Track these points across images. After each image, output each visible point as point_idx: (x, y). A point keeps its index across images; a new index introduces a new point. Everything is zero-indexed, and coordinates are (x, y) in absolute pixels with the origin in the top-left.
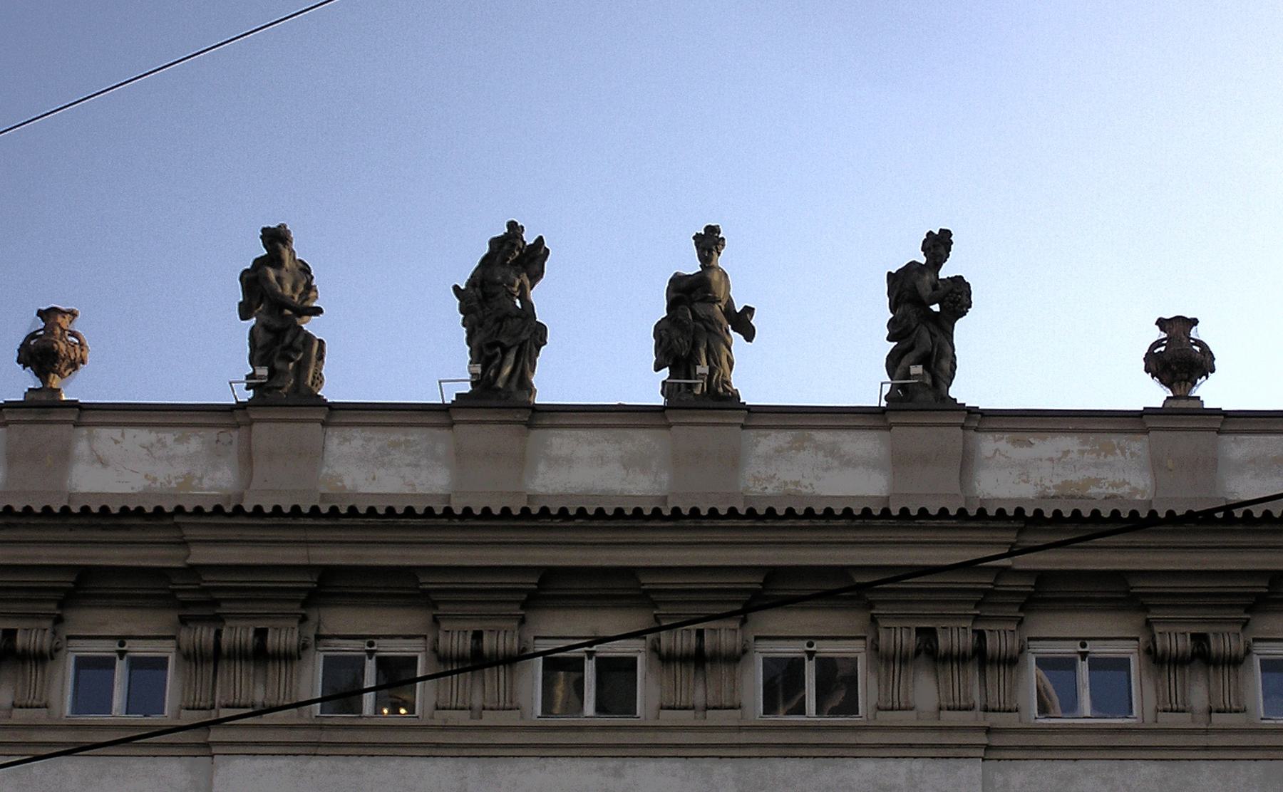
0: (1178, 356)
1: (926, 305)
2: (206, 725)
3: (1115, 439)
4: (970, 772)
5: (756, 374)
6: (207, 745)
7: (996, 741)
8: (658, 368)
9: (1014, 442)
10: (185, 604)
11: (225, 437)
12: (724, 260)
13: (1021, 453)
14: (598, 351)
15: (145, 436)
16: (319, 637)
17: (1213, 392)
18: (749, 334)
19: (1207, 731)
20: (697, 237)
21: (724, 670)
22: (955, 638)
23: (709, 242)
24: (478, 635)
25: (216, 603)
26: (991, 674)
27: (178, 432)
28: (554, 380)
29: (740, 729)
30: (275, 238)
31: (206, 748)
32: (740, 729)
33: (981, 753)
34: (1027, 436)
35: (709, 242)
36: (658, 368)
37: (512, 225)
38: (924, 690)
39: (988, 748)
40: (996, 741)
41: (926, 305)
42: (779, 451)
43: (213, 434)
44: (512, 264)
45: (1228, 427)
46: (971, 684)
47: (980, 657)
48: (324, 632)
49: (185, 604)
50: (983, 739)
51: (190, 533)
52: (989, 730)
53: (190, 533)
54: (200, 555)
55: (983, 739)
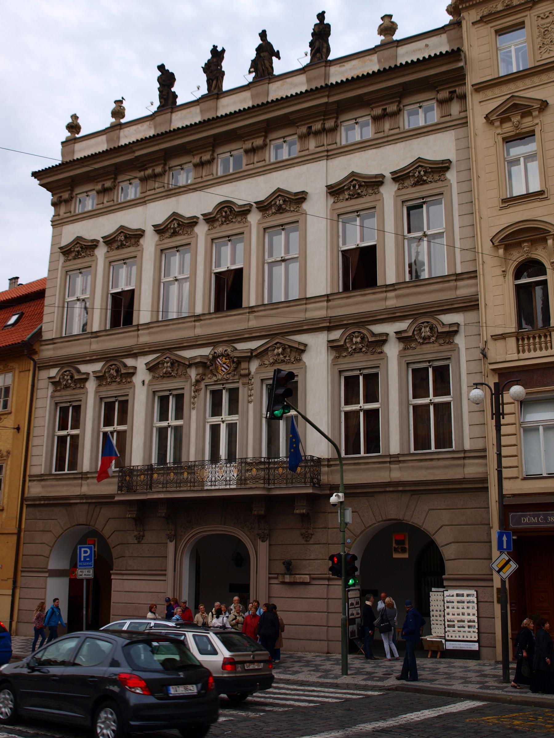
0: (388, 27)
1: (321, 33)
2: (145, 197)
3: (367, 58)
4: (323, 163)
5: (279, 67)
6: (145, 202)
7: (329, 153)
8: (250, 72)
9: (340, 66)
10: (140, 167)
11: (151, 123)
12: (269, 39)
13: (343, 69)
14: (237, 73)
15: (134, 128)
16: (170, 168)
17: (397, 36)
18: (279, 58)
19: (387, 136)
20: (260, 34)
21: (260, 151)
22: (317, 126)
23: (263, 35)
24: (201, 158)
25: (145, 165)
26: (329, 135)
27: (141, 125)
28: (227, 85)
29: (264, 166)
30: (161, 68)
31: (145, 203)
32: (264, 166)
33: (326, 158)
34: (343, 64)
35: (263, 35)
36: (250, 72)
37: (214, 46)
38: (312, 144)
39: (328, 156)
40: (329, 153)
41: (321, 33)
42: (278, 87)
43: (148, 123)
44: (217, 55)
45: (400, 44)
46: (325, 139)
47: (324, 131)
48: (170, 166)
49: (140, 167)
50: (325, 154)
51: (134, 149)
52: (327, 151)
53: (134, 149)
54: (138, 153)
55: (325, 154)
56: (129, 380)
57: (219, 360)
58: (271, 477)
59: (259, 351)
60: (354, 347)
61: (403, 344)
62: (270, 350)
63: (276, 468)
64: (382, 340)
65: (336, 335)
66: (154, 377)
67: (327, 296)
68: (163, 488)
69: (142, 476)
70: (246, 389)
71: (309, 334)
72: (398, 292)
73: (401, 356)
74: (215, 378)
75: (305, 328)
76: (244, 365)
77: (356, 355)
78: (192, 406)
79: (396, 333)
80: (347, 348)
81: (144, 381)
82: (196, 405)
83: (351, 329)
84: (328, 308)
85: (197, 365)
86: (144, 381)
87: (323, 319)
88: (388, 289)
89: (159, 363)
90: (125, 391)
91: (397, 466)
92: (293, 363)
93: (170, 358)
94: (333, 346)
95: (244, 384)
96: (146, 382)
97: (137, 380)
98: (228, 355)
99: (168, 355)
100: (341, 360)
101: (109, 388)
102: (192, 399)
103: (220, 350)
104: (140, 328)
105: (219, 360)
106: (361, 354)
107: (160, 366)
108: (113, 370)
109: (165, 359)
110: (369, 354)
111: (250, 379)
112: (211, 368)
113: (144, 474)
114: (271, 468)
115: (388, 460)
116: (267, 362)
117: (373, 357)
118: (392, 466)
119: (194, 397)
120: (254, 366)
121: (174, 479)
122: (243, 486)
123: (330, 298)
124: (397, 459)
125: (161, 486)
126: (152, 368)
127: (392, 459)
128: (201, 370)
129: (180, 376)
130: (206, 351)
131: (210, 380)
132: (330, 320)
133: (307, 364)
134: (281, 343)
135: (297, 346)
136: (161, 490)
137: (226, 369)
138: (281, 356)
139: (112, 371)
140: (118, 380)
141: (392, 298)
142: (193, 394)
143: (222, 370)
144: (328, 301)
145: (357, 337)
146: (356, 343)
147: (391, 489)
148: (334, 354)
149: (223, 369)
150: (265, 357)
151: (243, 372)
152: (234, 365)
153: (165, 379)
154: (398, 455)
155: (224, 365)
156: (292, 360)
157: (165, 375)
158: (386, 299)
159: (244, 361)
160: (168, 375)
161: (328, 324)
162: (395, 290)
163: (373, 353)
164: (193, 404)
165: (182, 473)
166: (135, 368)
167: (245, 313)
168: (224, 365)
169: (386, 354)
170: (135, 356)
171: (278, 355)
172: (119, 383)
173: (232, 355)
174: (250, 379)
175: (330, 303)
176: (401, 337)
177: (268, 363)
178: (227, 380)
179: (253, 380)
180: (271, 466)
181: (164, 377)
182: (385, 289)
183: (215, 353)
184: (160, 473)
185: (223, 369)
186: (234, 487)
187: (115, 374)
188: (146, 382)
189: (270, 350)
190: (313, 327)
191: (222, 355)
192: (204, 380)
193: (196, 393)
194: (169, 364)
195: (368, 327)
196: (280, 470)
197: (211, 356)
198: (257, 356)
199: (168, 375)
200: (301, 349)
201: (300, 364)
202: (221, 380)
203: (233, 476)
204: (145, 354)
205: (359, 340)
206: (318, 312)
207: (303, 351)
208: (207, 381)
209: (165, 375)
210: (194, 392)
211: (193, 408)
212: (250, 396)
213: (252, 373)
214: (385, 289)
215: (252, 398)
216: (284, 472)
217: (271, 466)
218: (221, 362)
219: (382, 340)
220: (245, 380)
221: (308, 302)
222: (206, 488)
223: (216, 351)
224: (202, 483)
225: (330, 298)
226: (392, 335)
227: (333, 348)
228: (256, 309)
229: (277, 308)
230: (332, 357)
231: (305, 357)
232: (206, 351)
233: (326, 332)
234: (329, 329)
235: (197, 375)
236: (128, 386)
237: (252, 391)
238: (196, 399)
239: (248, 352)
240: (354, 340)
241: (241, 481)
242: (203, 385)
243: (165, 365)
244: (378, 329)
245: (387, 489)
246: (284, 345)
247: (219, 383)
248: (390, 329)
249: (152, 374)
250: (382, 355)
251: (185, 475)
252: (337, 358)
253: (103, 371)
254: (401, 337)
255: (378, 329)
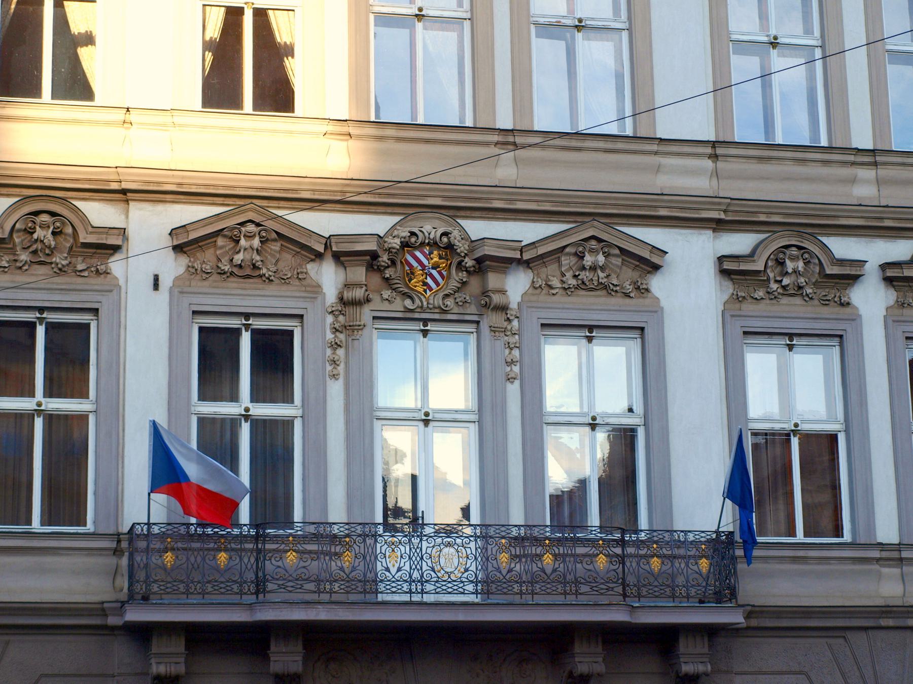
56: (102, 268)
57: (418, 254)
58: (631, 580)
59: (541, 250)
60: (786, 281)
61: (895, 293)
62: (569, 254)
63: (642, 557)
64: (849, 275)
65: (739, 243)
66: (192, 271)
67: (714, 144)
68: (319, 592)
69: (169, 557)
70: (500, 344)
71: (667, 230)
72: (883, 172)
73: (891, 319)
74: (408, 303)
75: (663, 212)
76: (493, 280)
77: (785, 300)
78: (329, 368)
79: (884, 267)
80: (768, 280)
81: (156, 279)
82: (341, 368)
83: (783, 237)
84: (716, 174)
85: (339, 258)
86: (156, 279)
87: (712, 200)
88: (860, 159)
89: (218, 233)
90: (83, 297)
91: (896, 571)
92: (627, 295)
93: (258, 225)
94: (729, 269)
95: (493, 330)
96: (166, 282)
97: (131, 271)
98: (450, 247)
99: (251, 216)
100: (748, 308)
101: (21, 278)
102: (329, 352)
103: (431, 228)
104: (133, 116)
105: (418, 254)
106: (798, 301)
107: (220, 241)
108: (44, 226)
109: (242, 224)
110: (816, 302)
111: (508, 320)
112: (388, 273)
113: (173, 549)
114: (631, 556)
115: (876, 554)
116: (555, 282)
117: (825, 311)
118: (886, 570)
119: (335, 346)
120: (516, 286)
121: (354, 569)
122: (494, 599)
123: (720, 151)
124: (895, 555)
125: (311, 586)
126: (185, 244)
127: (885, 554)
128: (359, 273)
129: (284, 281)
130: (378, 224)
131: (386, 306)
132: (729, 204)
133: (663, 303)
134: (599, 240)
135: (646, 254)
136: (315, 597)
137: (437, 284)
138: (601, 275)
139: (39, 233)
140: (60, 259)
141: (867, 182)
142: (330, 336)
143: (425, 284)
144: (714, 157)
145: (793, 259)
146: (795, 271)
147: (891, 622)
148: (729, 288)
149: (429, 281)
150: (552, 268)
151: (496, 299)
152: (457, 276)
153: (233, 283)
154: (899, 547)
155: (434, 272)
156: (629, 288)
157: (235, 270)
158: (853, 181)
159: (496, 270)
160: (248, 271)
161: (722, 216)
162: (875, 164)
163: (825, 302)
164: (334, 362)
165: (540, 556)
166: (123, 232)
167: (487, 144)
168: (434, 272)
169: (857, 308)
170: (124, 195)
171: (593, 268)
172: (61, 271)
173: (462, 247)
174: (508, 320)
175: (721, 165)
176: (894, 276)
177: (560, 286)
178: (445, 312)
179: (515, 323)
180: (630, 550)
181: (232, 274)
182: (852, 158)
183: (413, 234)
184: (310, 552)
185: (429, 280)
186: (472, 598)
187: (50, 239)
188: (166, 282)
189: (569, 254)
190: (685, 216)
191: (434, 244)
192: (368, 300)
193: (342, 336)
194: (256, 242)
195: (825, 240)
196: (655, 563)
197: (396, 243)
198: (527, 264)
199: (250, 273)
200: (649, 264)
201: (647, 301)
202: (428, 310)
203: (388, 569)
204: (154, 194)
205: (800, 265)
206: (691, 179)
207: (656, 268)
208: (376, 304)
209: (235, 270)
210: (335, 330)
211: (334, 376)
212: (511, 363)
213: (514, 305)
214: (852, 158)
215: (516, 369)
216: (664, 568)
217: (630, 550)
218: (425, 262)
219: (849, 275)
220: (497, 319)
221: (663, 148)
222: (380, 597)
223: (416, 230)
224: (368, 584)
225: (720, 151)
226: (871, 270)
227: (725, 273)
228: (519, 140)
229: (579, 149)
230: (726, 297)
231: (657, 284)
232: (378, 224)
233: (709, 233)
234: (719, 226)
235: (347, 286)
236: (97, 282)
237: (516, 352)
238: (341, 352)
239: (514, 250)
240: (790, 266)
241: (488, 585)
242: (366, 314)
243: (243, 242)
244: (843, 247)
245: (884, 622)
246: (611, 245)
247: (417, 316)
248: (875, 252)
249: (184, 261)
250: (847, 310)
251: (548, 559)
252: (737, 299)
253: (8, 227)
254: (894, 276)
255: (843, 247)
